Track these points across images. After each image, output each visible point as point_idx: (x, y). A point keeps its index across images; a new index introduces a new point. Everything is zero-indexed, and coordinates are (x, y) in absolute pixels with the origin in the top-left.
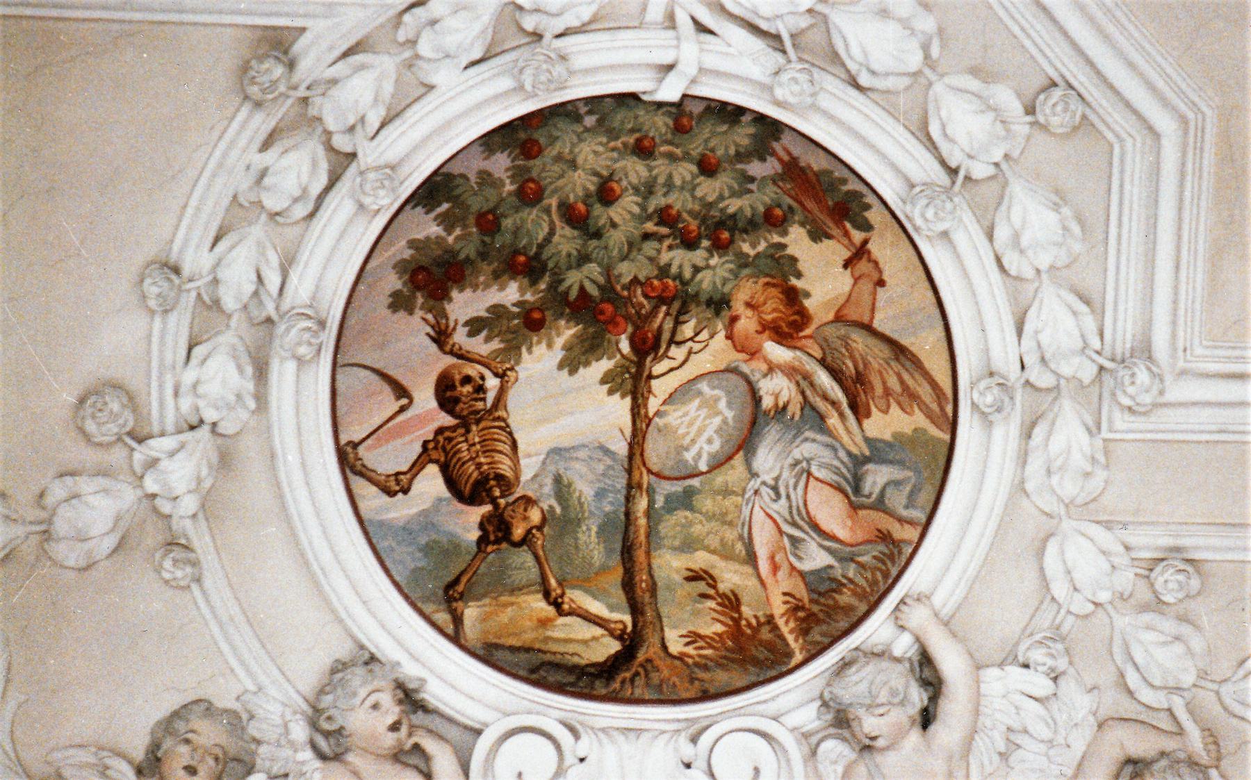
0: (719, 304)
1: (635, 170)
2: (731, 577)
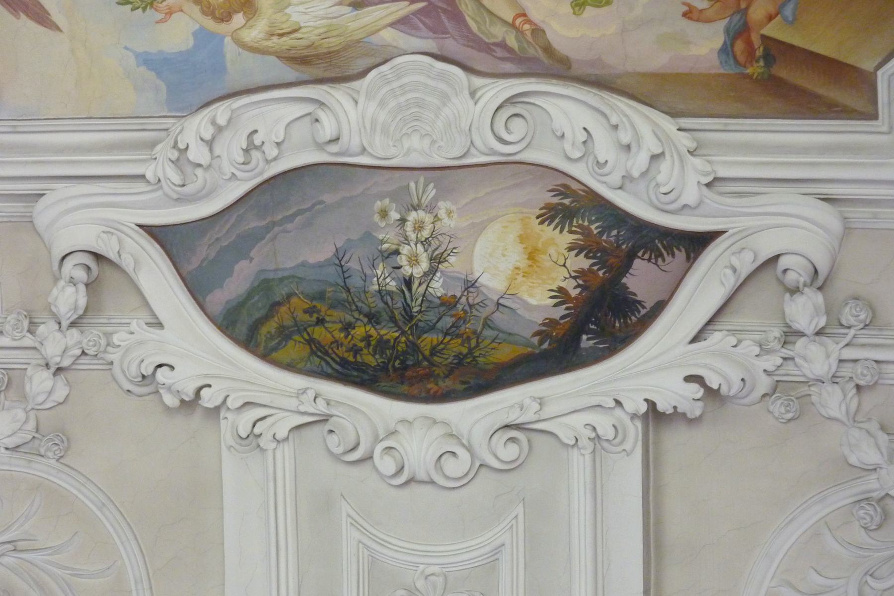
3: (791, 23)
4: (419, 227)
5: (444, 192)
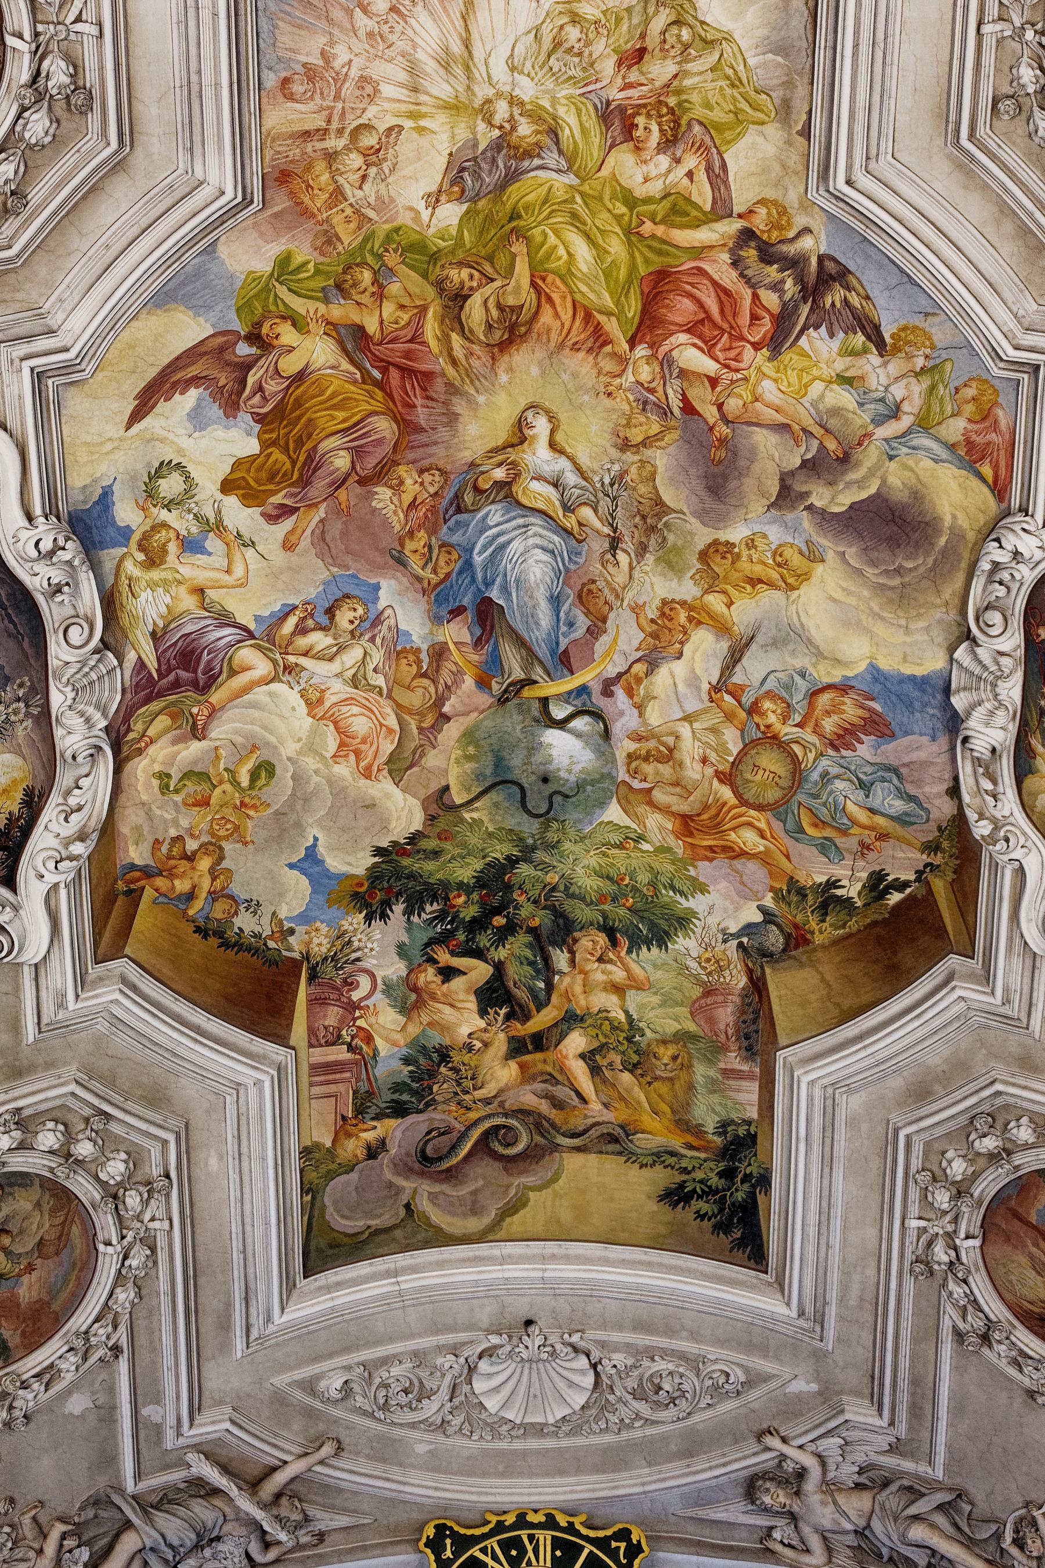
3: (154, 902)
4: (16, 712)
5: (37, 720)
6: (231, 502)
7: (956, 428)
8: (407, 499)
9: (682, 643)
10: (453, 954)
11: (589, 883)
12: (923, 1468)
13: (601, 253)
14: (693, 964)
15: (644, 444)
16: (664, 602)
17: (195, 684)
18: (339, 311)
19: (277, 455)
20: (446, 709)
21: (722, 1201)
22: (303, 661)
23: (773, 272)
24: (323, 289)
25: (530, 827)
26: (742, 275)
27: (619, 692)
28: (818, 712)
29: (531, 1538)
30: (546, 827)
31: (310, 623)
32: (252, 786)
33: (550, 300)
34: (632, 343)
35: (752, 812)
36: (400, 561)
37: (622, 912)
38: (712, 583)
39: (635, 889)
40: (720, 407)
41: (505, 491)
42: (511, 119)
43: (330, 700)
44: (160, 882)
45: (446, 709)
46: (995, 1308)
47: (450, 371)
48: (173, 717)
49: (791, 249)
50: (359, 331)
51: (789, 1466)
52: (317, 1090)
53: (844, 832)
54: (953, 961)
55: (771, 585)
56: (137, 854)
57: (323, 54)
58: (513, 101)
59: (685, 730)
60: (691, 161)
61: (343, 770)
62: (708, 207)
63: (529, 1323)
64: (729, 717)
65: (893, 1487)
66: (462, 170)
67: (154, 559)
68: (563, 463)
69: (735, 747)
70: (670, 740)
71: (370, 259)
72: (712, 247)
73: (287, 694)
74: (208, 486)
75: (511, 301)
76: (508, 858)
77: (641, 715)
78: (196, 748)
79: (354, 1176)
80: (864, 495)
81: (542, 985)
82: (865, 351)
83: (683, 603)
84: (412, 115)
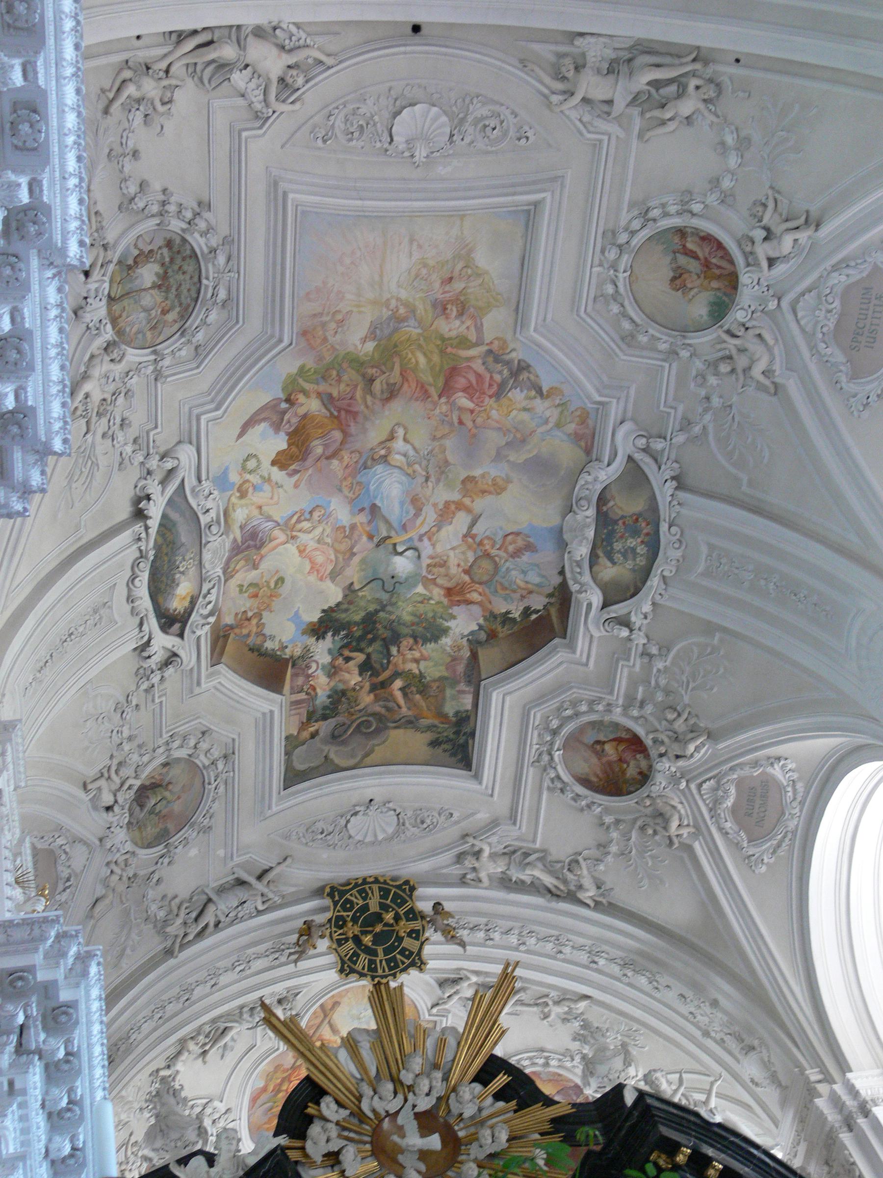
0: (167, 298)
1: (187, 277)
2: (124, 315)
3: (234, 639)
6: (275, 469)
7: (571, 427)
8: (345, 464)
9: (452, 518)
10: (351, 651)
11: (407, 618)
12: (531, 845)
13: (429, 360)
14: (448, 649)
15: (441, 438)
16: (446, 502)
17: (255, 546)
18: (323, 387)
19: (294, 449)
20: (354, 550)
21: (454, 745)
22: (299, 534)
23: (499, 367)
24: (317, 379)
25: (385, 597)
26: (486, 368)
27: (425, 539)
28: (507, 543)
29: (370, 888)
30: (392, 596)
31: (302, 518)
32: (275, 588)
33: (407, 380)
34: (440, 396)
35: (477, 586)
36: (340, 490)
37: (420, 629)
38: (466, 493)
39: (427, 620)
40: (474, 421)
41: (385, 459)
42: (397, 307)
43: (309, 549)
44: (237, 631)
45: (354, 550)
46: (566, 777)
47: (366, 411)
48: (246, 561)
49: (507, 357)
50: (330, 396)
51: (477, 849)
52: (293, 712)
53: (514, 591)
54: (557, 641)
55: (490, 493)
56: (229, 620)
57: (323, 282)
58: (398, 299)
59: (451, 554)
60: (469, 323)
61: (312, 578)
62: (474, 341)
63: (371, 800)
64: (470, 547)
65: (519, 853)
66: (376, 328)
67: (243, 494)
68: (409, 447)
69: (471, 560)
70: (445, 558)
71: (336, 366)
72: (474, 357)
73: (292, 548)
74: (266, 463)
75: (392, 381)
76: (376, 610)
77: (434, 548)
78: (254, 573)
79: (305, 746)
80: (531, 455)
81: (385, 661)
82: (535, 398)
83: (453, 502)
84: (358, 306)
